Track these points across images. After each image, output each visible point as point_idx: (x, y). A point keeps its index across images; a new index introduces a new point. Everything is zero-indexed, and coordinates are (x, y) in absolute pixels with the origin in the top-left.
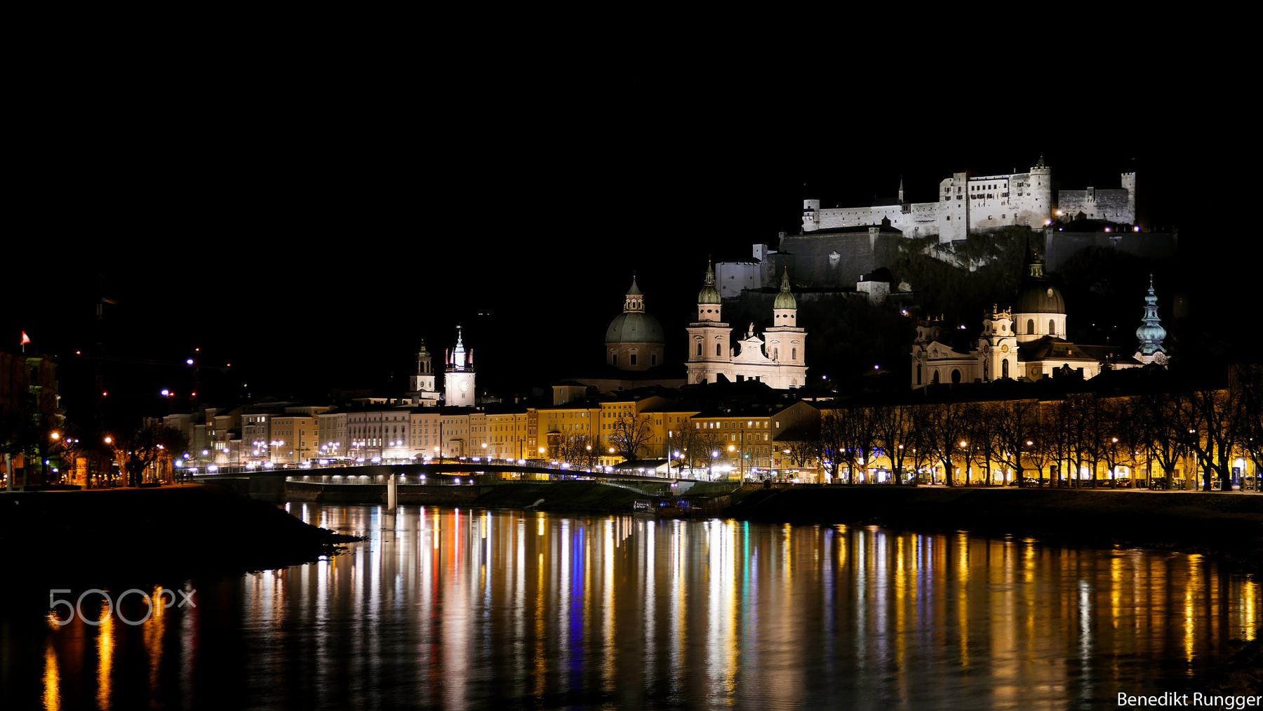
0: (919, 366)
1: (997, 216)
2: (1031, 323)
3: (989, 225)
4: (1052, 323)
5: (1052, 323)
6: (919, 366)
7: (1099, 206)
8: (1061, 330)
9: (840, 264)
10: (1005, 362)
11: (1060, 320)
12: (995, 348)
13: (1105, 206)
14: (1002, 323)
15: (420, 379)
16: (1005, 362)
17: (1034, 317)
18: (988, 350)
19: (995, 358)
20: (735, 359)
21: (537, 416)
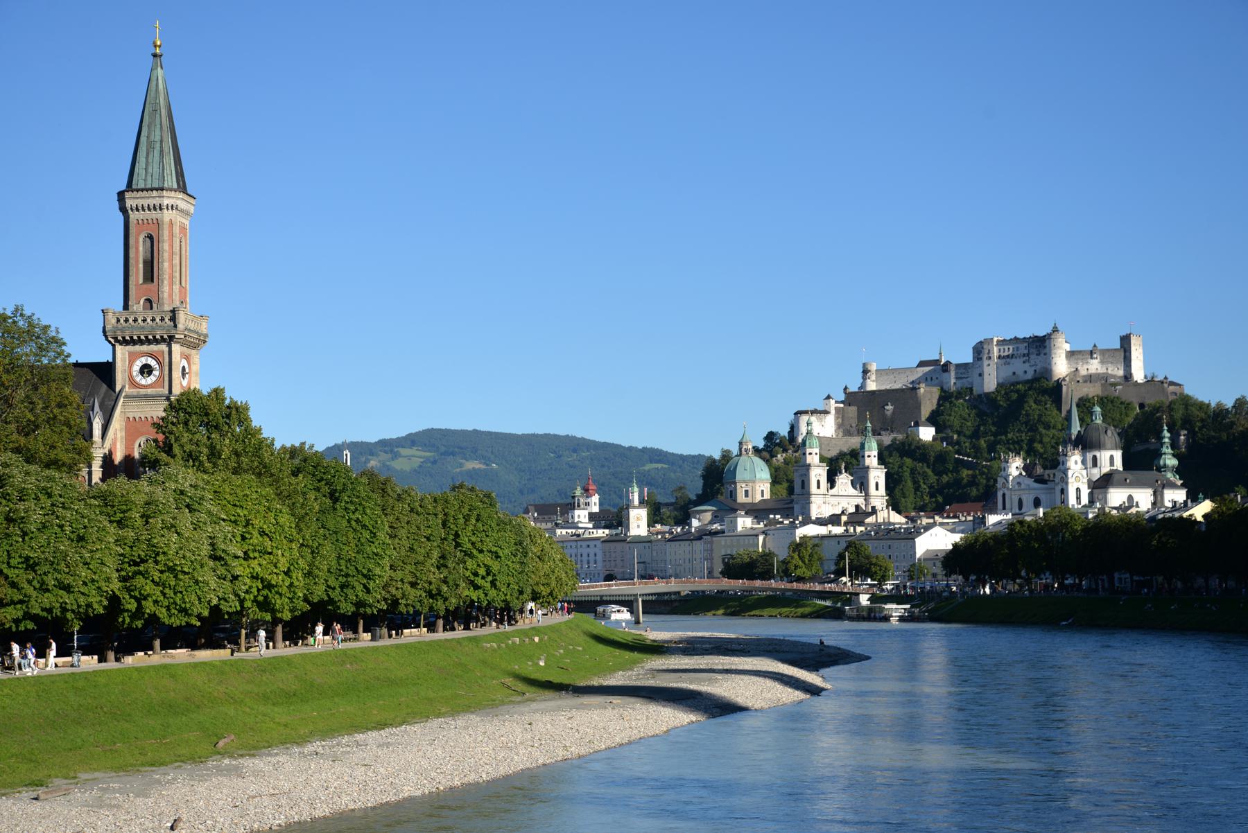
0: (1004, 495)
1: (1020, 373)
2: (1095, 458)
3: (1014, 379)
4: (1112, 458)
5: (1112, 458)
6: (1004, 495)
7: (1102, 362)
8: (1119, 465)
9: (894, 413)
10: (1078, 490)
11: (1118, 455)
12: (1070, 480)
13: (1108, 362)
14: (1074, 461)
15: (577, 512)
16: (1078, 490)
17: (1097, 454)
18: (1065, 480)
19: (1070, 486)
20: (833, 492)
21: (711, 543)
